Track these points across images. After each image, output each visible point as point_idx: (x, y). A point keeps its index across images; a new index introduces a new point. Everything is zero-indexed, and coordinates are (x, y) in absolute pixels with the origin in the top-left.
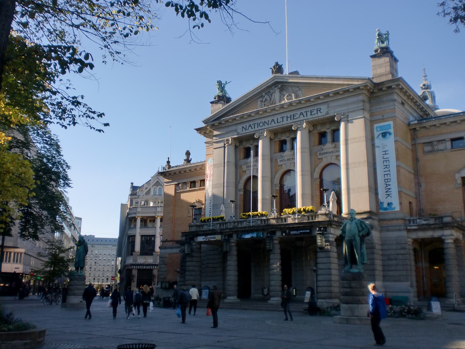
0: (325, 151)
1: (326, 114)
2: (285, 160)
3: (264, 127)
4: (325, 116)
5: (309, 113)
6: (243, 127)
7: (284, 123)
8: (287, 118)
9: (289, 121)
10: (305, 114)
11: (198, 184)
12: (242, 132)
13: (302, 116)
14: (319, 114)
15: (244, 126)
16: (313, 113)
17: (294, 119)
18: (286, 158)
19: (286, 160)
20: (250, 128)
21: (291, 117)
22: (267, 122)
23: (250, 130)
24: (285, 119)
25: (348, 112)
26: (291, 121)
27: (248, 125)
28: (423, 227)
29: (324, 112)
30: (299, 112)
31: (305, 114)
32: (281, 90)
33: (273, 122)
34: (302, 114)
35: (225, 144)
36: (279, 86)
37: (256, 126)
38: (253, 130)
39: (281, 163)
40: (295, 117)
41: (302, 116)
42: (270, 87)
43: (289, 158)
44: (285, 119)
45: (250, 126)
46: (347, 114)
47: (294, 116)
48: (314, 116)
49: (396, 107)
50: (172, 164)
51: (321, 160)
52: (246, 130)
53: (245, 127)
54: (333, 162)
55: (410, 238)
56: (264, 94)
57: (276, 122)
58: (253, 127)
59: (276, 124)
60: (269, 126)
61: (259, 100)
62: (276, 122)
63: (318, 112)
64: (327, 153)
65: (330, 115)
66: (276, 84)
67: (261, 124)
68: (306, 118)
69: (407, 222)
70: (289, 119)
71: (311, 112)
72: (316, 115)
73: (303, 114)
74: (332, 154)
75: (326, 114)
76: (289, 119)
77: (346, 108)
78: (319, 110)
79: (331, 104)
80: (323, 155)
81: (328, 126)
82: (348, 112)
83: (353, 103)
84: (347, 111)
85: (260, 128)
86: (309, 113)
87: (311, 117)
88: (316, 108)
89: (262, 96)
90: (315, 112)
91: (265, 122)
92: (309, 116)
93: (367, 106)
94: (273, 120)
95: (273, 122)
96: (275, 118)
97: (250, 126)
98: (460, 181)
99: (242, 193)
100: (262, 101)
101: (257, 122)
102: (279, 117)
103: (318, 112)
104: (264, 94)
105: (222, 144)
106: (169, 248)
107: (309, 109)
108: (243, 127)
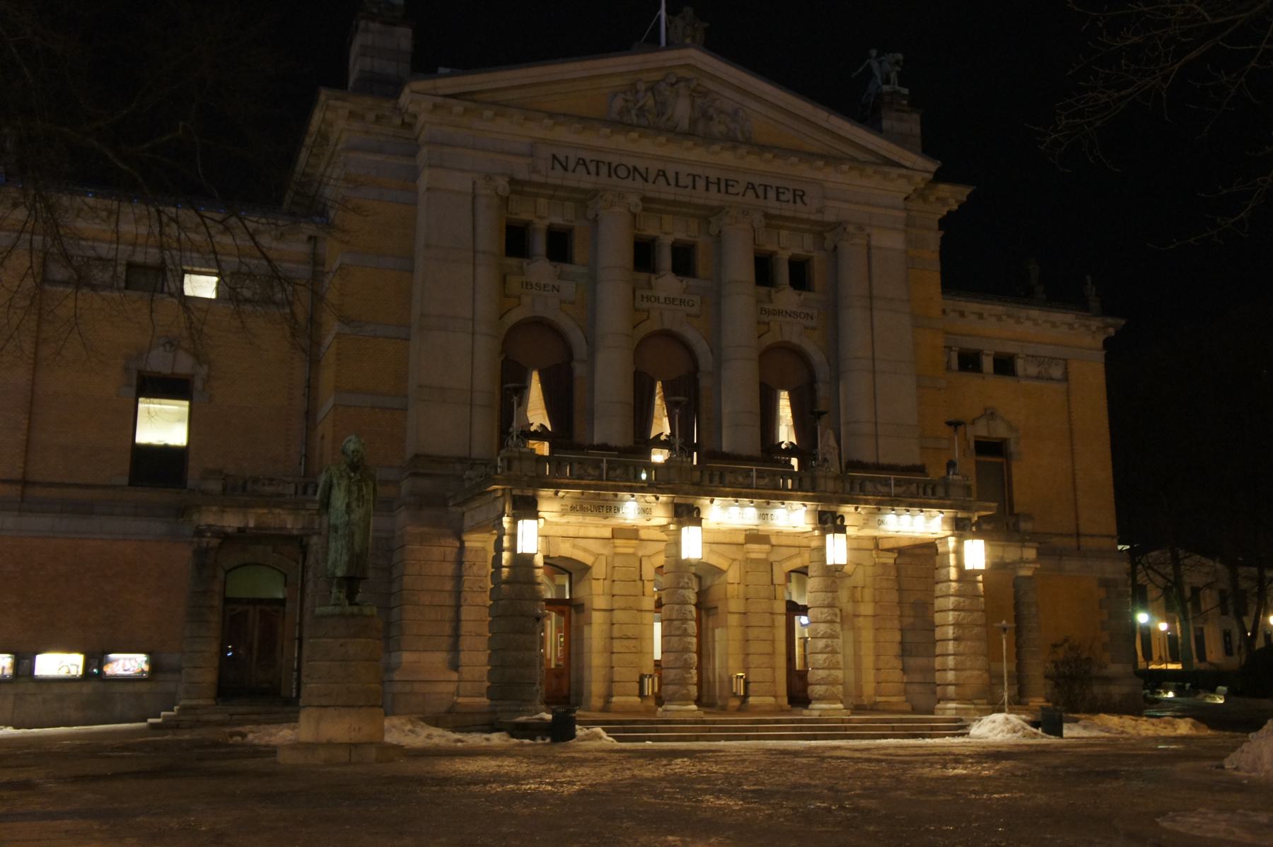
2: (657, 299)
5: (772, 194)
8: (708, 183)
13: (750, 193)
18: (662, 296)
19: (662, 300)
21: (719, 184)
31: (761, 193)
37: (604, 170)
47: (727, 185)
52: (566, 169)
62: (672, 182)
63: (798, 199)
70: (713, 188)
71: (778, 193)
76: (713, 188)
90: (789, 196)
91: (635, 169)
95: (662, 180)
98: (972, 445)
103: (798, 199)
108: (554, 157)
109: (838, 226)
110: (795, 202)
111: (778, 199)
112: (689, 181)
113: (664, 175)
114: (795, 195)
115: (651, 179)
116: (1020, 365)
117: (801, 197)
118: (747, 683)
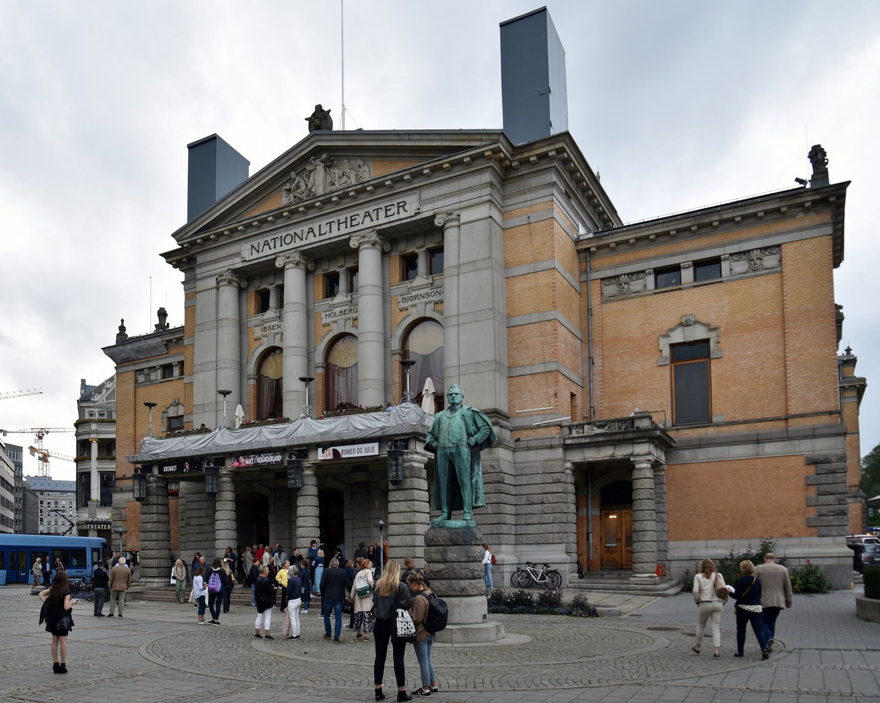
0: (414, 294)
1: (416, 214)
3: (293, 245)
4: (413, 219)
5: (382, 214)
6: (252, 246)
7: (332, 235)
8: (339, 224)
9: (343, 231)
10: (374, 216)
11: (176, 371)
12: (252, 257)
13: (368, 219)
14: (403, 215)
15: (255, 245)
16: (389, 213)
17: (352, 226)
18: (337, 310)
19: (338, 314)
20: (266, 247)
21: (346, 222)
22: (299, 233)
23: (267, 251)
24: (335, 227)
25: (460, 209)
26: (347, 231)
27: (262, 242)
28: (596, 440)
29: (411, 207)
30: (362, 213)
33: (311, 234)
34: (367, 214)
35: (218, 283)
38: (273, 251)
39: (328, 320)
40: (354, 223)
41: (368, 219)
43: (343, 308)
44: (335, 227)
45: (267, 243)
46: (458, 212)
47: (352, 220)
48: (391, 219)
49: (555, 199)
50: (131, 333)
51: (405, 313)
53: (256, 245)
54: (429, 314)
55: (569, 461)
57: (317, 233)
58: (272, 245)
59: (318, 238)
60: (304, 242)
62: (317, 233)
63: (401, 209)
64: (416, 296)
65: (424, 215)
67: (288, 240)
68: (375, 223)
69: (566, 431)
70: (343, 226)
71: (386, 211)
73: (369, 215)
74: (426, 300)
75: (416, 214)
76: (343, 226)
77: (456, 199)
78: (402, 206)
79: (427, 194)
80: (410, 303)
81: (419, 243)
82: (460, 209)
84: (458, 206)
85: (285, 247)
86: (382, 214)
87: (387, 220)
88: (395, 202)
89: (291, 180)
90: (394, 210)
91: (295, 234)
92: (383, 220)
93: (498, 198)
94: (311, 230)
95: (311, 234)
97: (267, 243)
99: (252, 382)
101: (279, 235)
102: (323, 222)
103: (401, 209)
105: (212, 282)
107: (383, 206)
108: (252, 246)
109: (434, 217)
110: (398, 213)
111: (386, 216)
113: (313, 231)
114: (399, 207)
115: (304, 237)
116: (725, 266)
117: (403, 206)
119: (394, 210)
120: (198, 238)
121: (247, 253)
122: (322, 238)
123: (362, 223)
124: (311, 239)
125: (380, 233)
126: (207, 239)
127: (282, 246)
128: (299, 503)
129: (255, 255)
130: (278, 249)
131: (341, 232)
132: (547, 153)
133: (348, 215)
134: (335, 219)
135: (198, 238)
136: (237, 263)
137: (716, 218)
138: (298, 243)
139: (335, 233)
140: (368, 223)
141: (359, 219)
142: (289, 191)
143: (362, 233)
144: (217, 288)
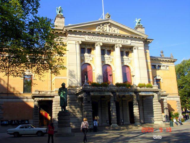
5: (123, 42)
9: (113, 42)
12: (88, 40)
23: (92, 40)
24: (111, 40)
29: (129, 42)
32: (110, 26)
36: (109, 24)
38: (94, 40)
42: (105, 23)
43: (107, 58)
44: (111, 40)
56: (101, 25)
59: (107, 42)
61: (98, 27)
66: (108, 23)
70: (113, 41)
72: (126, 43)
76: (113, 41)
83: (141, 44)
88: (125, 40)
90: (125, 42)
92: (123, 43)
94: (105, 39)
96: (106, 38)
100: (99, 28)
104: (101, 25)
105: (74, 42)
106: (5, 98)
109: (133, 47)
112: (110, 40)
115: (104, 40)
116: (161, 67)
118: (124, 120)
119: (125, 42)
120: (73, 30)
121: (87, 38)
122: (108, 42)
123: (119, 42)
124: (105, 41)
125: (122, 45)
126: (74, 31)
127: (100, 41)
128: (60, 102)
129: (89, 40)
130: (96, 40)
131: (113, 42)
132: (137, 37)
133: (115, 39)
134: (112, 39)
135: (73, 30)
136: (84, 40)
137: (162, 59)
138: (102, 41)
139: (111, 42)
140: (119, 42)
141: (118, 41)
142: (99, 28)
143: (119, 44)
144: (76, 45)
